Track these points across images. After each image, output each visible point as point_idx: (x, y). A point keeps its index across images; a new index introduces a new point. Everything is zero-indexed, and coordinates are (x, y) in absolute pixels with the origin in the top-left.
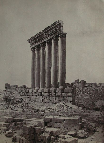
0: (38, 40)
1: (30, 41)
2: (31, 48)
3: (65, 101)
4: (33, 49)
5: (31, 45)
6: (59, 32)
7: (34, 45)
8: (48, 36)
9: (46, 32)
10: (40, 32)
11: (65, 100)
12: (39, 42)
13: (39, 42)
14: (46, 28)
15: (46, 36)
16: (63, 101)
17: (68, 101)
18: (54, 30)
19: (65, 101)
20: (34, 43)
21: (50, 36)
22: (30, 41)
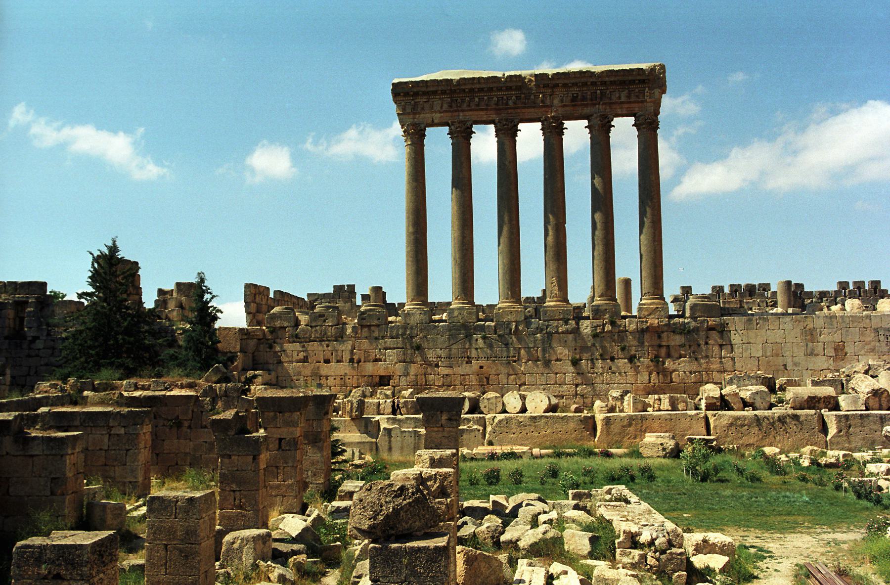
7: (438, 115)
8: (556, 102)
12: (481, 113)
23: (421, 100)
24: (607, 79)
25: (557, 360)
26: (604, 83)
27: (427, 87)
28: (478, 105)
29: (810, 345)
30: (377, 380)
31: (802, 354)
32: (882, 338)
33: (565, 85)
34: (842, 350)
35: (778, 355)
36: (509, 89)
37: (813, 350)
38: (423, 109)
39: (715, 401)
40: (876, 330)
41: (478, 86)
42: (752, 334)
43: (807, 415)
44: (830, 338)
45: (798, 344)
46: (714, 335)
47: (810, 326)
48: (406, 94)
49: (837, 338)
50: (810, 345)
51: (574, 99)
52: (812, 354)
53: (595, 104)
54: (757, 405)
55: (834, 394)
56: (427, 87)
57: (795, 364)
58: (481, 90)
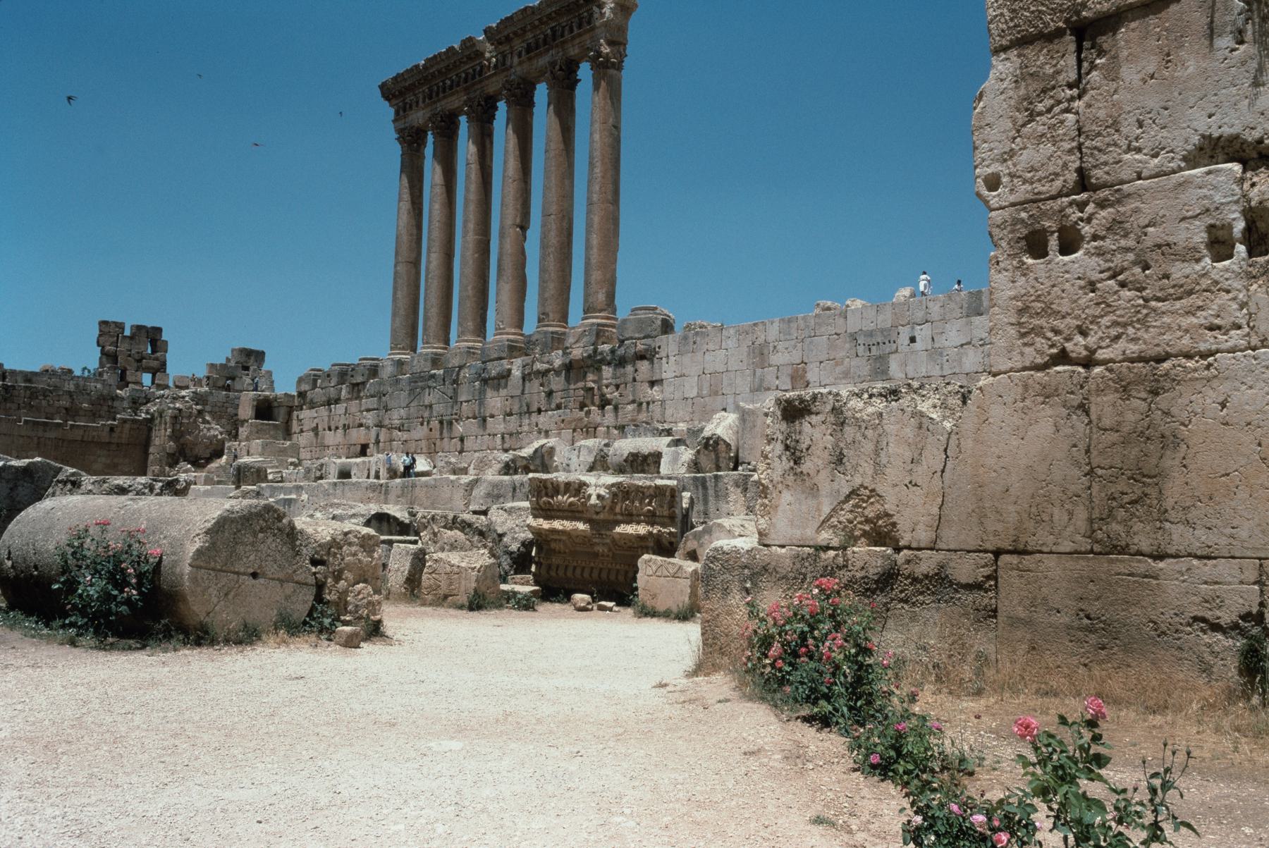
0: (448, 82)
1: (398, 92)
2: (400, 131)
3: (617, 387)
4: (411, 140)
5: (397, 113)
6: (587, 37)
7: (420, 114)
8: (516, 60)
9: (508, 39)
10: (470, 39)
11: (618, 381)
13: (453, 94)
14: (507, 18)
15: (504, 64)
16: (607, 387)
17: (634, 380)
18: (552, 29)
19: (617, 387)
20: (417, 102)
21: (530, 59)
22: (398, 92)
23: (410, 98)
24: (549, 10)
25: (492, 416)
26: (549, 17)
27: (405, 80)
28: (451, 87)
29: (759, 371)
30: (359, 448)
32: (861, 349)
33: (515, 33)
34: (803, 377)
35: (716, 393)
36: (470, 58)
37: (762, 380)
38: (411, 107)
40: (854, 337)
41: (442, 65)
42: (686, 359)
46: (644, 366)
47: (761, 340)
48: (394, 96)
50: (759, 371)
51: (529, 50)
53: (548, 50)
56: (405, 80)
58: (448, 69)
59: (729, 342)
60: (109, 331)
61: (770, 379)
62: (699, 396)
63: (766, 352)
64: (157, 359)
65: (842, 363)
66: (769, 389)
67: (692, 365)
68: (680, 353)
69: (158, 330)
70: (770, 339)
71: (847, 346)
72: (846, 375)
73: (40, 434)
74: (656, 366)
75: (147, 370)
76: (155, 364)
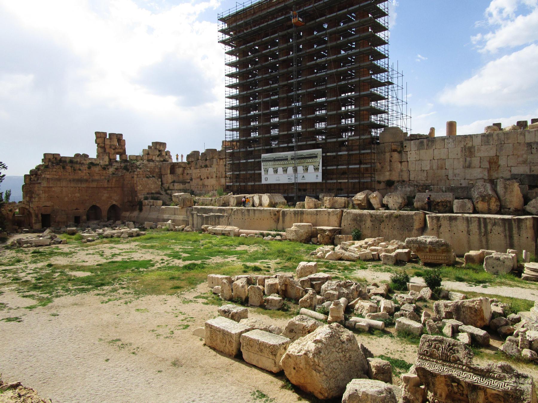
17: (391, 161)
29: (468, 159)
31: (461, 167)
34: (496, 163)
35: (442, 168)
39: (359, 202)
40: (530, 145)
42: (422, 152)
43: (408, 216)
44: (486, 154)
45: (458, 159)
46: (396, 155)
47: (470, 144)
49: (492, 153)
50: (468, 159)
52: (469, 167)
54: (390, 206)
55: (451, 199)
57: (455, 175)
59: (449, 145)
60: (100, 137)
61: (476, 161)
62: (431, 168)
63: (472, 150)
64: (121, 149)
65: (522, 156)
66: (475, 168)
67: (427, 154)
68: (419, 149)
69: (121, 135)
70: (475, 144)
71: (526, 148)
72: (525, 162)
73: (79, 186)
74: (404, 155)
75: (118, 153)
76: (121, 151)
